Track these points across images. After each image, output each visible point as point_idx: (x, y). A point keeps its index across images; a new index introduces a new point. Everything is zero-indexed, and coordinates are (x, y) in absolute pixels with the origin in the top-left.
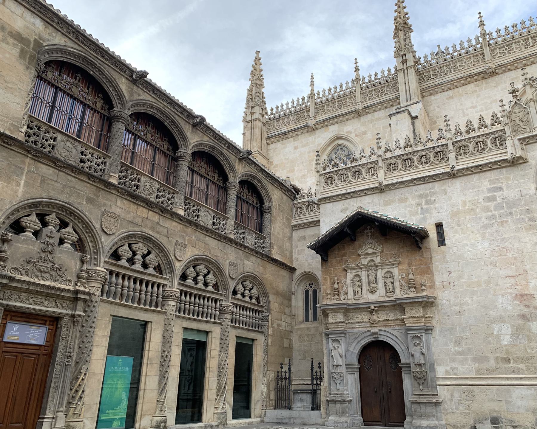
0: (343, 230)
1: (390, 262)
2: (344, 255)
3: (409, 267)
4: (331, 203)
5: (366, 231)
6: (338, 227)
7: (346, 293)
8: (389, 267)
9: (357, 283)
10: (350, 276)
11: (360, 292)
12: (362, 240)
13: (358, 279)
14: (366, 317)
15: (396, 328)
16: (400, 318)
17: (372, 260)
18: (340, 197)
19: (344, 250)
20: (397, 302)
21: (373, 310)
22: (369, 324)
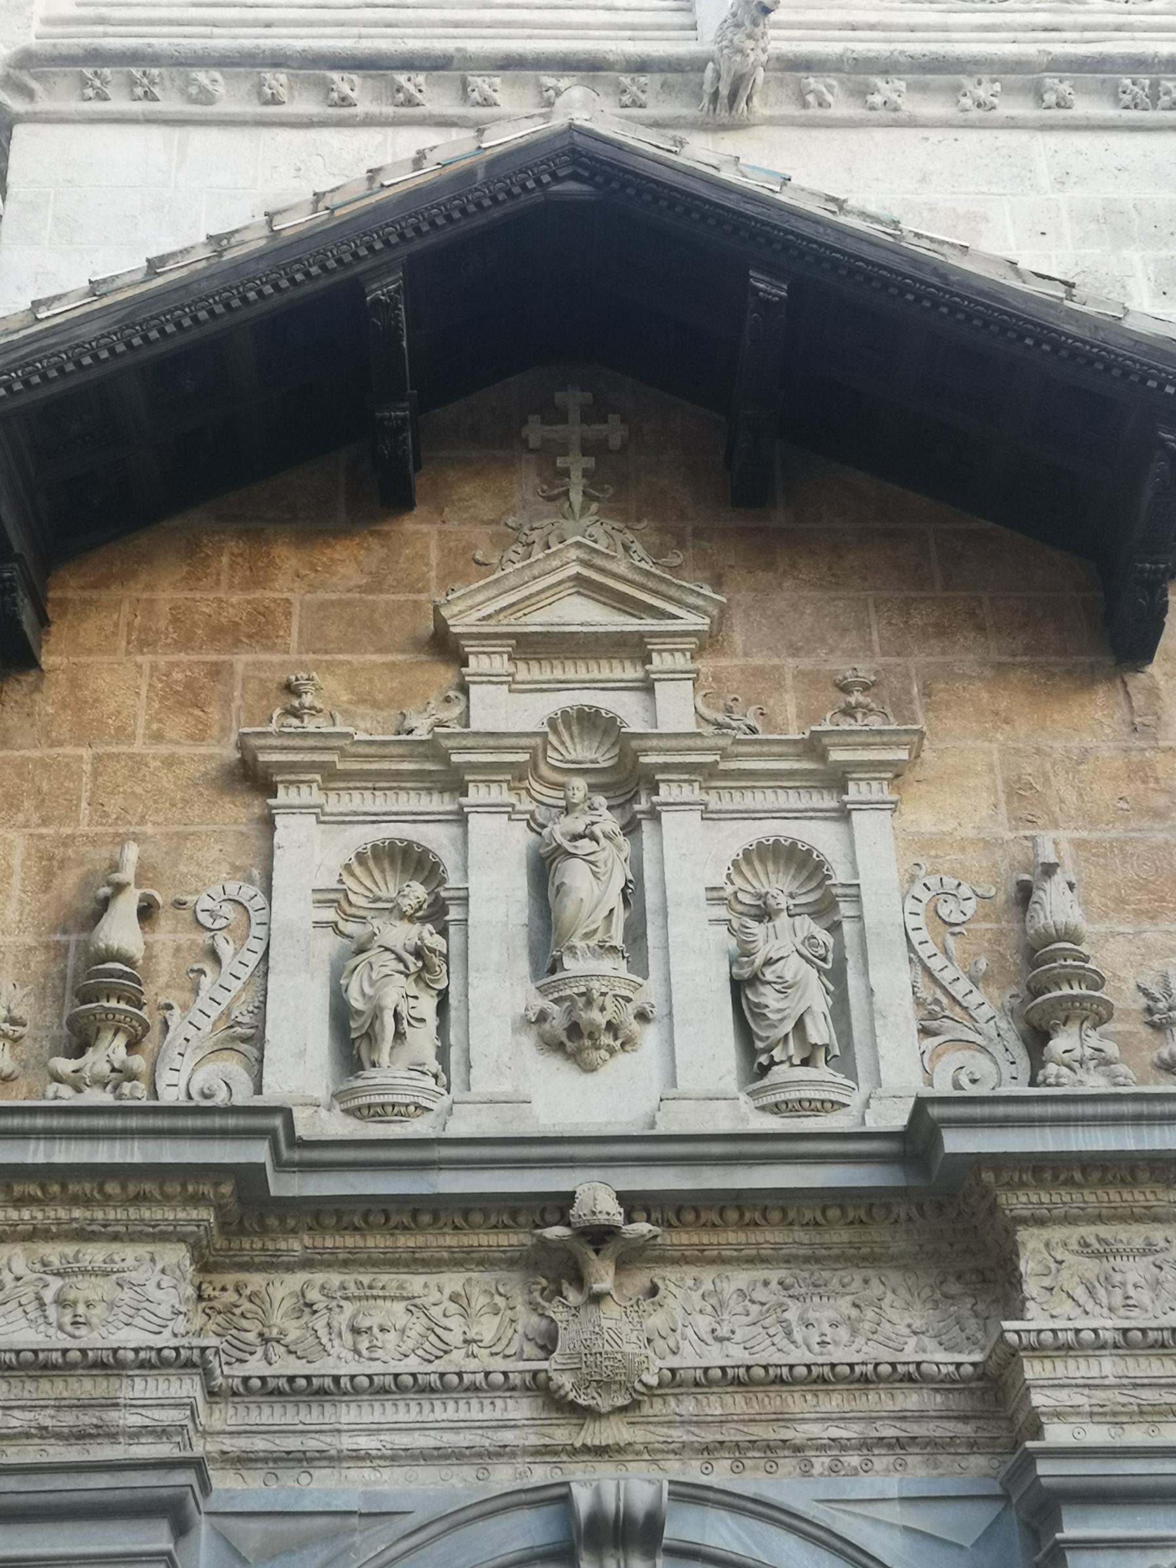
0: (354, 288)
1: (813, 747)
2: (261, 628)
3: (1018, 821)
4: (157, 134)
5: (535, 432)
6: (305, 238)
7: (248, 1039)
8: (792, 801)
9: (401, 934)
10: (313, 847)
11: (423, 1040)
12: (486, 507)
13: (418, 892)
14: (487, 1328)
15: (866, 1486)
16: (938, 1358)
17: (590, 722)
18: (278, 79)
19: (256, 581)
20: (955, 1142)
21: (600, 1236)
22: (521, 1409)
